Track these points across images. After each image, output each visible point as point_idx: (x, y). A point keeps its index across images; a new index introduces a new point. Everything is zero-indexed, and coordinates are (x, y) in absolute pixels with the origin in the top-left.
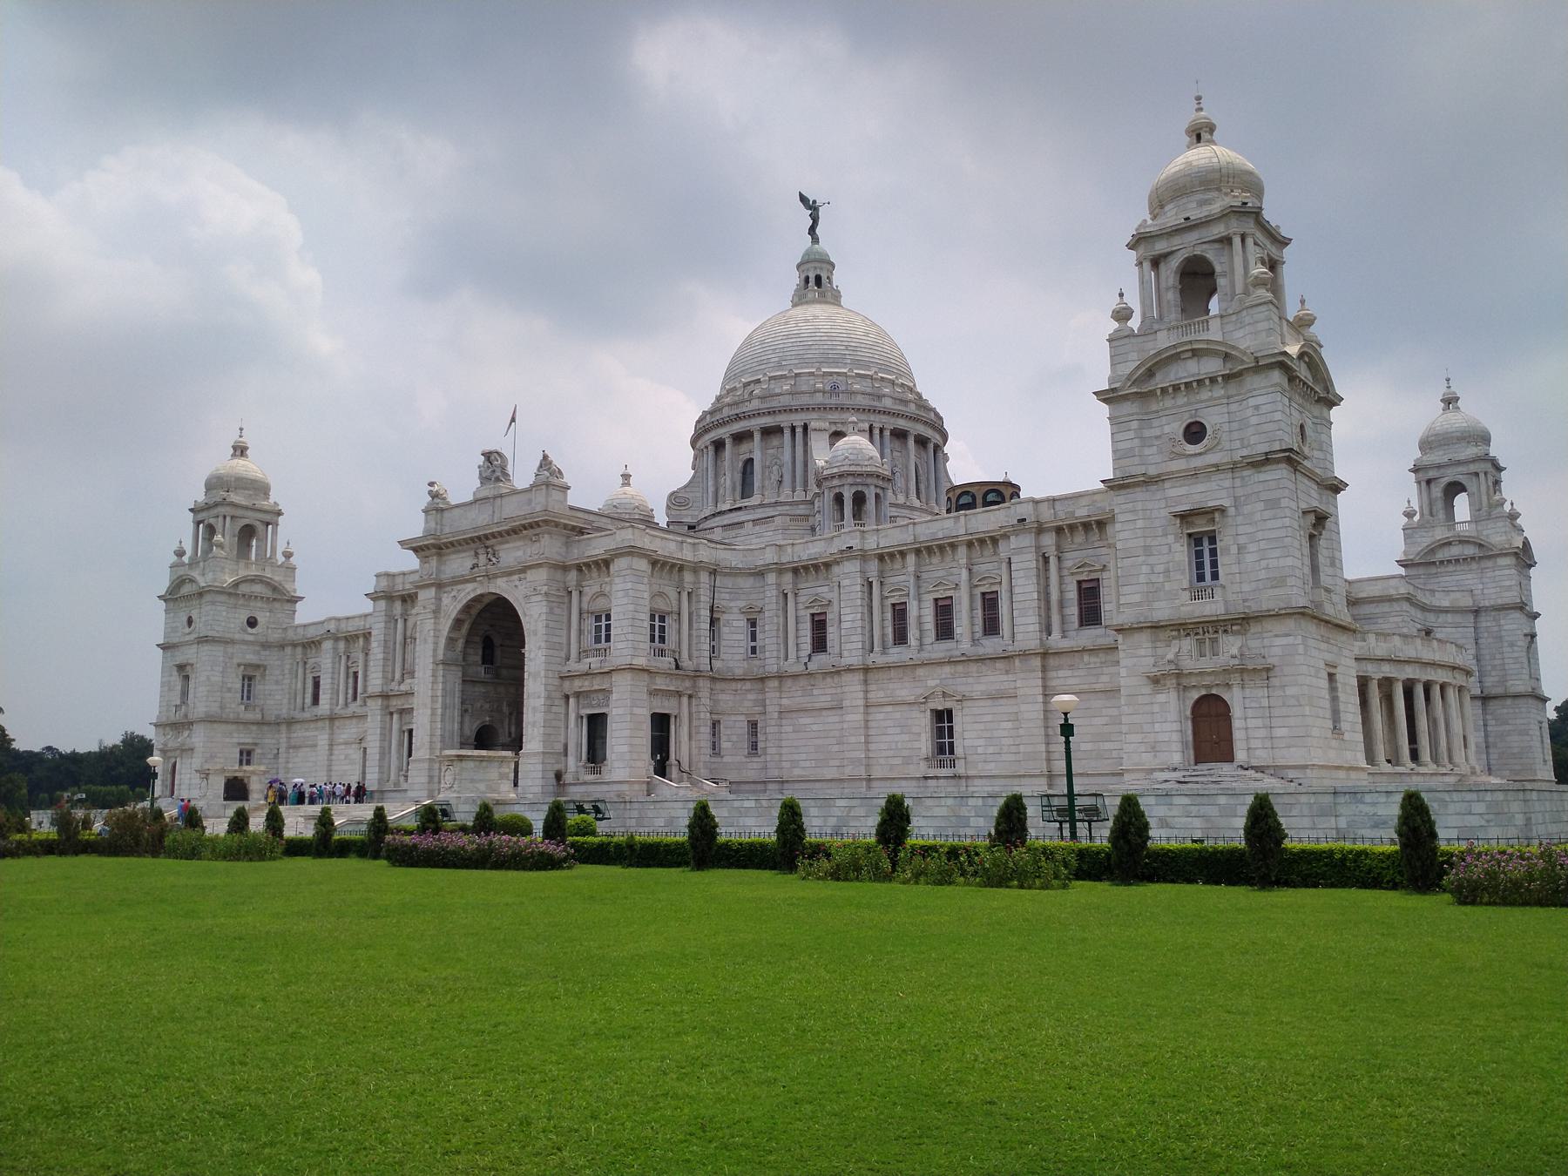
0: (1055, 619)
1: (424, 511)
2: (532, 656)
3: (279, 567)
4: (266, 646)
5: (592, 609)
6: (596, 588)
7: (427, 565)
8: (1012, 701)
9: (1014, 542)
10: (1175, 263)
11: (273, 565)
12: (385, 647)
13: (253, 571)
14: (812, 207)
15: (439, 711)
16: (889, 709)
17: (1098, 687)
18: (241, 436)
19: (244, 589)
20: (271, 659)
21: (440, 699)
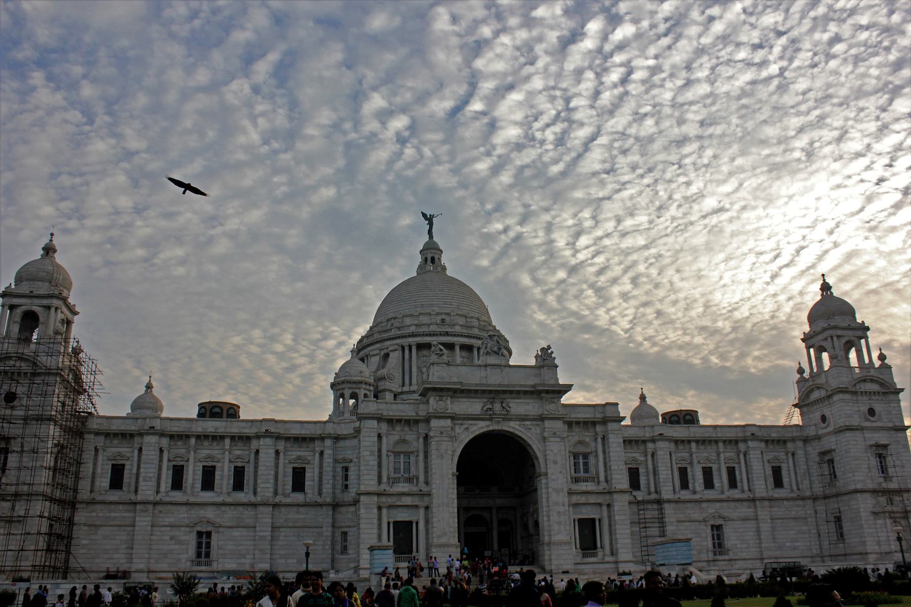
0: (768, 483)
2: (554, 477)
6: (576, 438)
7: (441, 403)
8: (753, 522)
9: (750, 444)
10: (844, 340)
14: (429, 219)
16: (688, 524)
17: (792, 516)
18: (51, 241)
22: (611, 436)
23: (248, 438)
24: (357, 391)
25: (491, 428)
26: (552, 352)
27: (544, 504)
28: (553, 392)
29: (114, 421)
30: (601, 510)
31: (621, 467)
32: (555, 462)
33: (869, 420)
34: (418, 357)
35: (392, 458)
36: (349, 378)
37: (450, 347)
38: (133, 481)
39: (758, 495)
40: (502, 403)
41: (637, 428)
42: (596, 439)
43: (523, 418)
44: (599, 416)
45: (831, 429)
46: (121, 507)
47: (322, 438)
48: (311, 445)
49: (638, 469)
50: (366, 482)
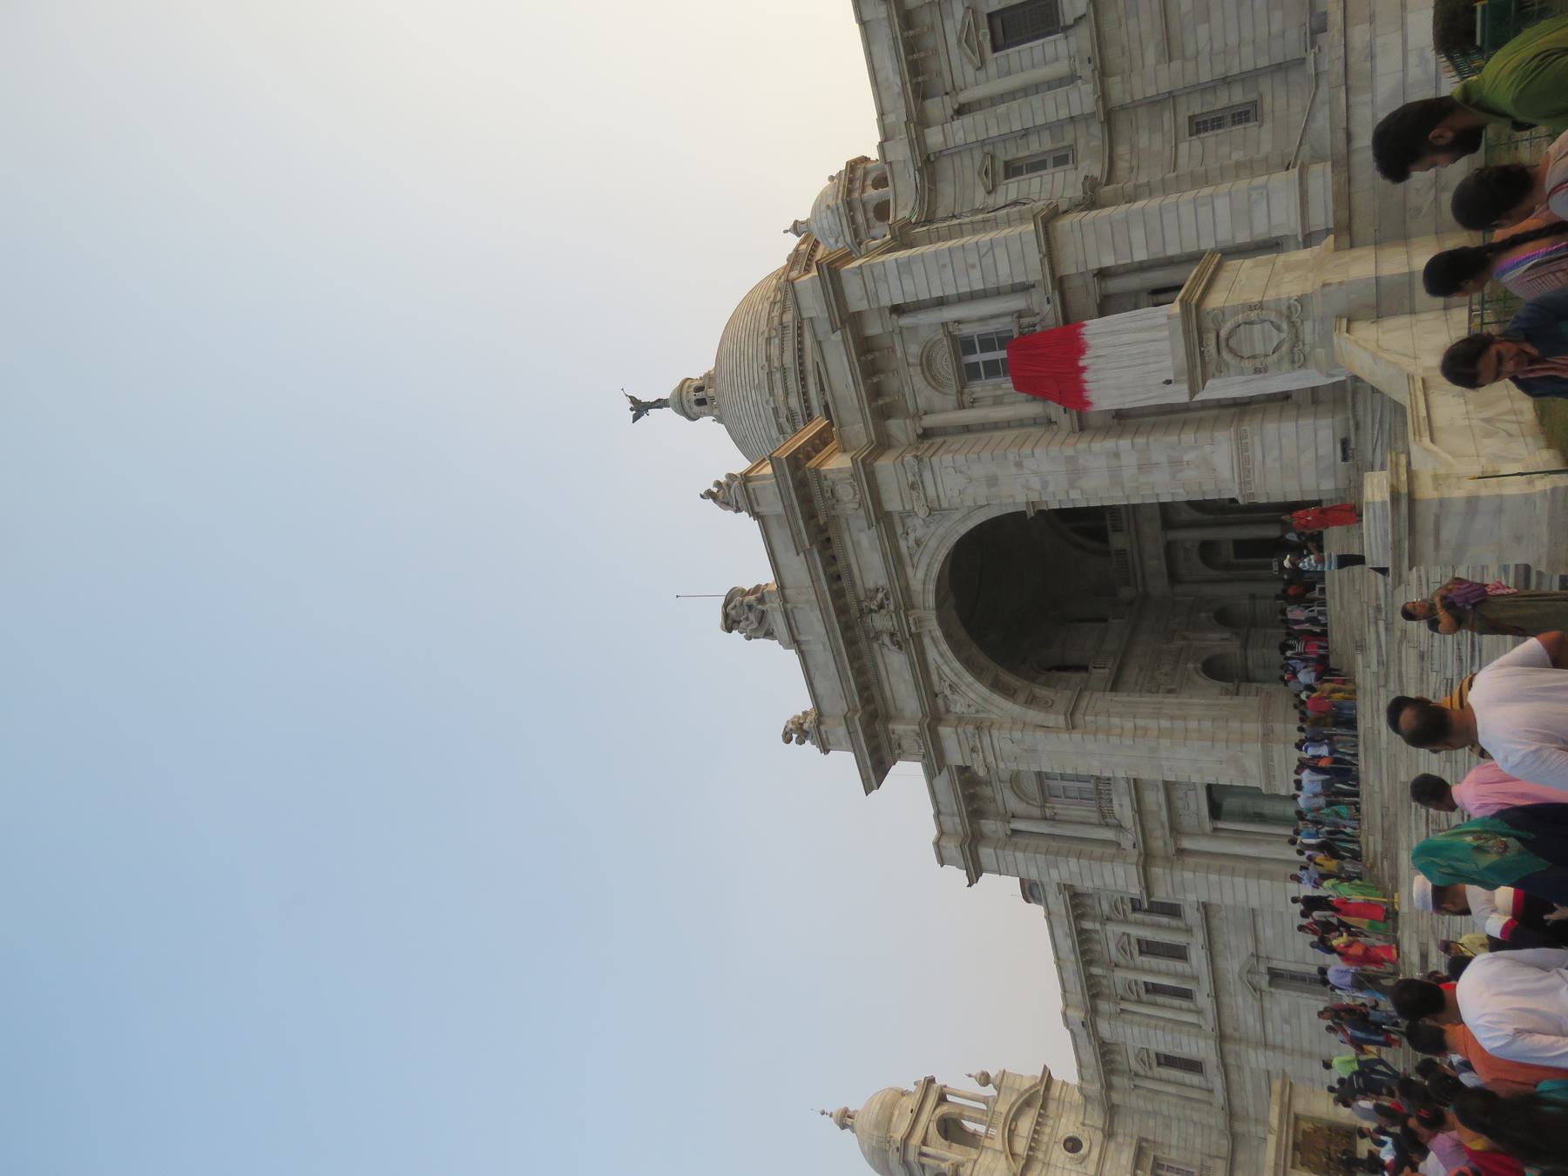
1: (826, 751)
2: (1036, 483)
3: (999, 1094)
4: (1109, 1134)
5: (953, 383)
6: (919, 382)
7: (905, 744)
11: (996, 1100)
12: (1057, 853)
13: (997, 1132)
14: (640, 408)
15: (1165, 723)
18: (831, 1116)
19: (1021, 1146)
20: (1129, 1129)
21: (1140, 722)
22: (886, 301)
25: (938, 633)
26: (718, 484)
28: (806, 500)
29: (1083, 1057)
31: (973, 258)
32: (992, 481)
35: (1060, 808)
40: (871, 611)
41: (875, 49)
43: (896, 561)
46: (1234, 1076)
49: (990, 16)
50: (1121, 882)
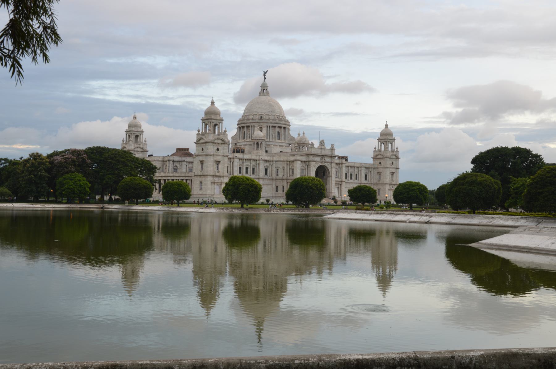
9: (362, 168)
18: (213, 99)
23: (256, 160)
24: (262, 142)
25: (321, 164)
27: (330, 183)
30: (339, 185)
33: (391, 165)
34: (272, 130)
36: (261, 138)
37: (280, 127)
38: (231, 171)
39: (362, 182)
42: (339, 168)
44: (341, 162)
45: (382, 166)
47: (273, 161)
48: (269, 162)
